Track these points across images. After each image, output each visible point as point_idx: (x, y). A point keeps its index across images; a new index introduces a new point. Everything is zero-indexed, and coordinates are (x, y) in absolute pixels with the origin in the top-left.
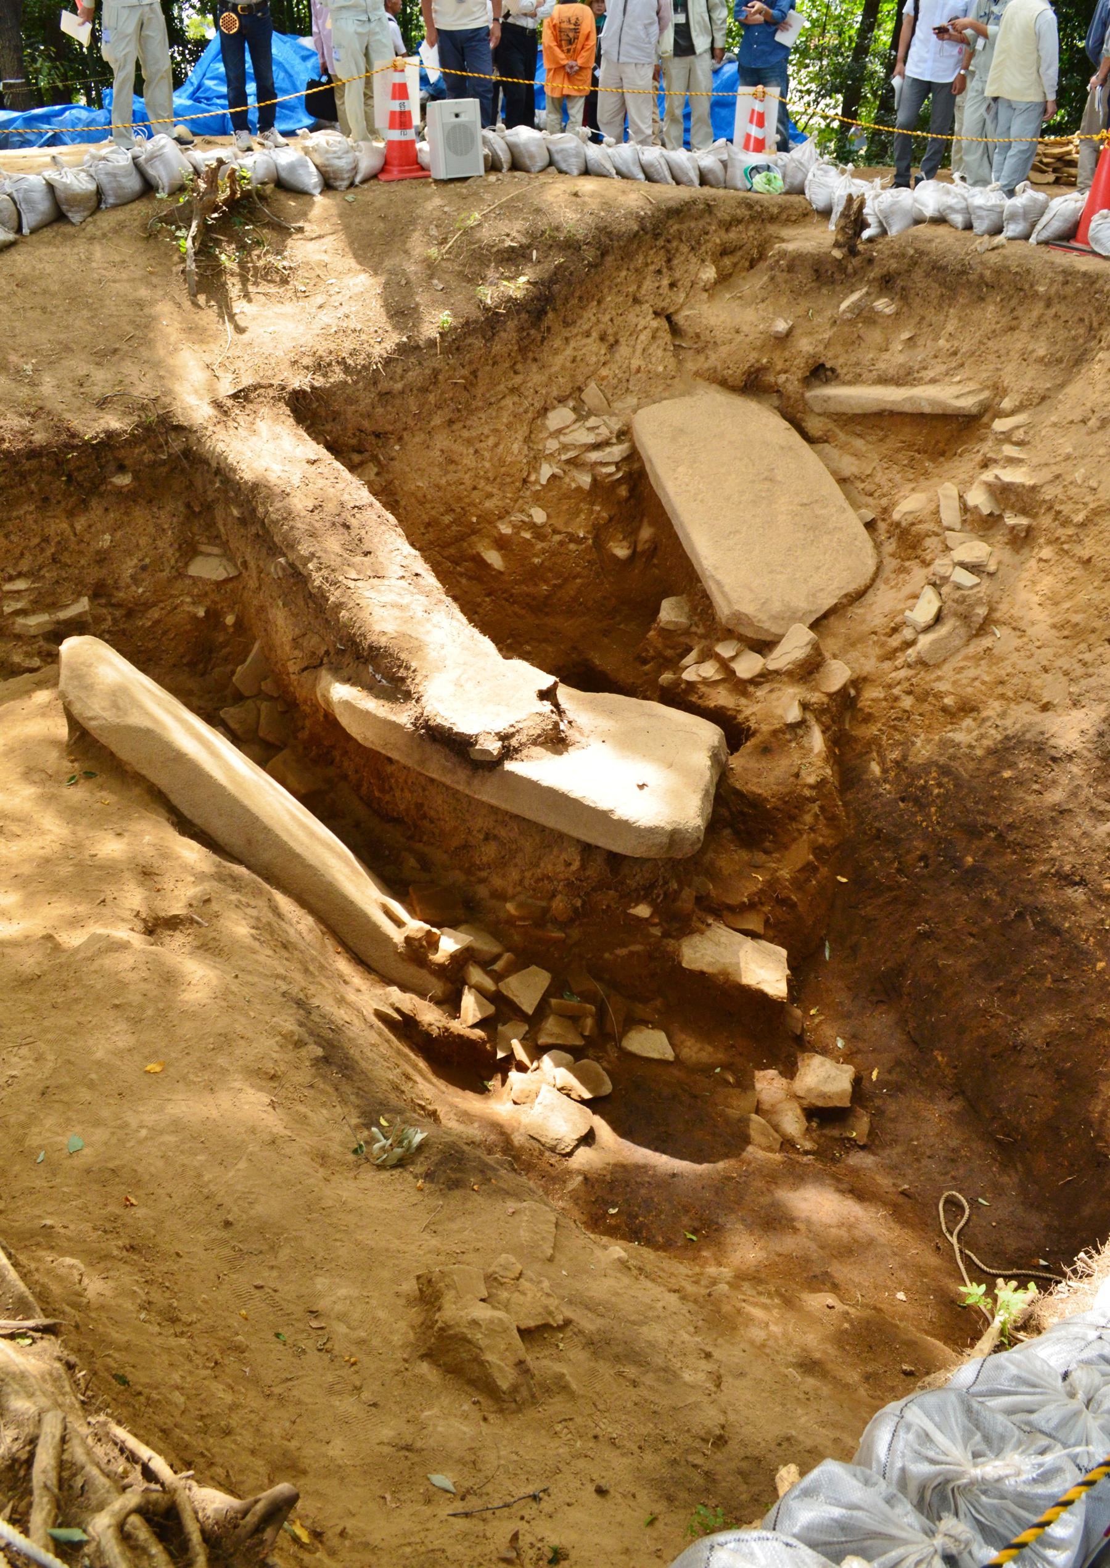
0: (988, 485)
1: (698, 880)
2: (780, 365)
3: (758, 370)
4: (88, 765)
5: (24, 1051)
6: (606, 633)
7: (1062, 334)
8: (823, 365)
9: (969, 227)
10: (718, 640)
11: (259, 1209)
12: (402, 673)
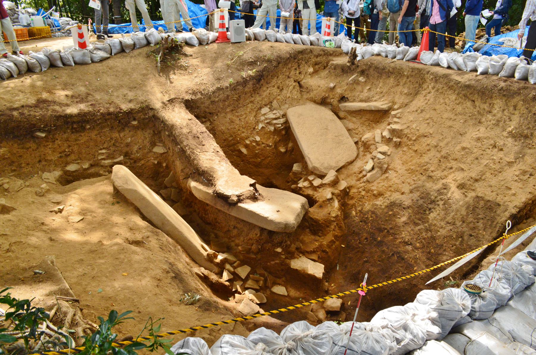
0: (389, 130)
1: (297, 243)
2: (331, 97)
3: (325, 98)
4: (118, 200)
5: (89, 267)
6: (278, 174)
7: (412, 86)
8: (344, 97)
9: (387, 56)
10: (309, 175)
11: (149, 309)
12: (211, 178)
